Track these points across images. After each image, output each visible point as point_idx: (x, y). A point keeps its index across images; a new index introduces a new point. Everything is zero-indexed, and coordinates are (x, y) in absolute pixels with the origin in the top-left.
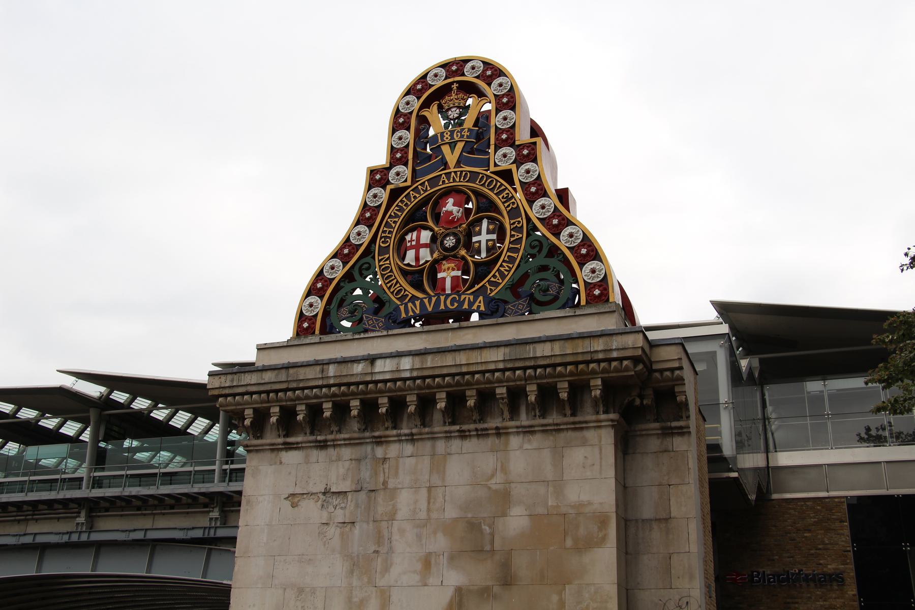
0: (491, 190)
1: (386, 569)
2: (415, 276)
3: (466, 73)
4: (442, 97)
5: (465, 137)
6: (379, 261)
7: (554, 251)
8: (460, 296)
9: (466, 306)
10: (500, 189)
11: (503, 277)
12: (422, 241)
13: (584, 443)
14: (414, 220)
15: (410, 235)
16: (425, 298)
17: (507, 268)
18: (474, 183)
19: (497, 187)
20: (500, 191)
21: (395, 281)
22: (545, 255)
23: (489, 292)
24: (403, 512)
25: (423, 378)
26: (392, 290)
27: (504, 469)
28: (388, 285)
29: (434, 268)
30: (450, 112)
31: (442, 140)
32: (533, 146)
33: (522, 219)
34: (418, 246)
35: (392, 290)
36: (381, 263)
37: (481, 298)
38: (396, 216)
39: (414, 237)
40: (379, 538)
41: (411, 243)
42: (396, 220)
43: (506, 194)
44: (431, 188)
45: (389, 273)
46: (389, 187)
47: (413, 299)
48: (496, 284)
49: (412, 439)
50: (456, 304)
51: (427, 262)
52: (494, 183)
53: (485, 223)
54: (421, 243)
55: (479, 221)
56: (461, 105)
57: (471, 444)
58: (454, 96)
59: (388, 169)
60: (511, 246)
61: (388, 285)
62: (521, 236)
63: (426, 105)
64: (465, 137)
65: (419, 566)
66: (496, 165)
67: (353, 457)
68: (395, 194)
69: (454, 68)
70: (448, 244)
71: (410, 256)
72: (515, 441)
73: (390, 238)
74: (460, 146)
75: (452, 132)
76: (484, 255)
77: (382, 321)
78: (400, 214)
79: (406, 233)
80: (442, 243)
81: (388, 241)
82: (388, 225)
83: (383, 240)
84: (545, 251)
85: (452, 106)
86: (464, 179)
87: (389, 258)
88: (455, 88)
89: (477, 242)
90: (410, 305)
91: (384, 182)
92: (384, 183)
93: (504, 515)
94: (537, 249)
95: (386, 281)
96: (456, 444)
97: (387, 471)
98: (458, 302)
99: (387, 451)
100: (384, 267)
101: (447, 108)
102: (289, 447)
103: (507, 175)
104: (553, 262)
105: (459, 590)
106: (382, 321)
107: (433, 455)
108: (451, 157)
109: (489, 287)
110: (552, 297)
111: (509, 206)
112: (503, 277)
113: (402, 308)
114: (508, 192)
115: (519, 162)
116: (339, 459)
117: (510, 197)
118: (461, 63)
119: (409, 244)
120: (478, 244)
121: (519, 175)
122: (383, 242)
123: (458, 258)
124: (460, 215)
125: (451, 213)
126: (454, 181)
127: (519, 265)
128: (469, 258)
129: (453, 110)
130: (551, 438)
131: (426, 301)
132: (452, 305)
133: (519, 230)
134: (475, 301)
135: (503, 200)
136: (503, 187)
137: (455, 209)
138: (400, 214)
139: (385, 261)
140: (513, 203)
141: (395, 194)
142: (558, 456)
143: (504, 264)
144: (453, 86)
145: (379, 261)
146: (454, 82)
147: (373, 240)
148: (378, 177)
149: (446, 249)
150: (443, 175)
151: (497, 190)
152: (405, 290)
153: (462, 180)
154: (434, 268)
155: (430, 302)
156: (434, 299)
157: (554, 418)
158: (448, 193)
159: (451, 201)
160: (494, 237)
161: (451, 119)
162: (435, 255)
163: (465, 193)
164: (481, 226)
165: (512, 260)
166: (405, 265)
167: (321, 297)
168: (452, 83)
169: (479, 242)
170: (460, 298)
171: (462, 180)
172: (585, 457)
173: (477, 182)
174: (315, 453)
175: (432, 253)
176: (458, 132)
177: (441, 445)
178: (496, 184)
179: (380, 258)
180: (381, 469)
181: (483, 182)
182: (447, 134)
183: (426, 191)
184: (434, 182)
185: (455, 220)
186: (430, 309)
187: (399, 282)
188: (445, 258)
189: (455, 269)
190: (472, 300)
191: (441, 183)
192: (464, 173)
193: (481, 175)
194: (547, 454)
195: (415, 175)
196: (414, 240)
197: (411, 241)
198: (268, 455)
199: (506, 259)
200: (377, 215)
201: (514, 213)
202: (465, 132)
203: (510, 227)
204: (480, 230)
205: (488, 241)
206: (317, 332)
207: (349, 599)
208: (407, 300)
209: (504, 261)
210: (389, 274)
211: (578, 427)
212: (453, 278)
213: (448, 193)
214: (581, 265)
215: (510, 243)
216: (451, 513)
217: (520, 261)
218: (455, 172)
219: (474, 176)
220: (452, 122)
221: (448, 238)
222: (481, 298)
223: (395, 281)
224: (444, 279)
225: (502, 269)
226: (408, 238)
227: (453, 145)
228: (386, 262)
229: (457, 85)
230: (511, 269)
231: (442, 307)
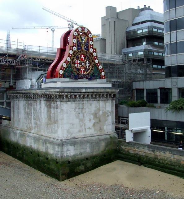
1: (84, 121)
7: (98, 69)
11: (91, 72)
13: (108, 102)
24: (87, 112)
27: (99, 106)
34: (78, 63)
40: (84, 116)
49: (87, 101)
55: (87, 61)
57: (95, 102)
65: (89, 120)
68: (74, 52)
71: (76, 65)
72: (100, 102)
74: (84, 46)
80: (81, 64)
82: (73, 58)
93: (99, 112)
96: (93, 102)
102: (69, 101)
103: (92, 54)
105: (94, 123)
107: (90, 103)
108: (83, 47)
128: (86, 68)
133: (93, 64)
141: (74, 52)
147: (71, 61)
149: (82, 65)
157: (105, 99)
159: (83, 56)
160: (89, 64)
165: (92, 69)
174: (73, 102)
177: (91, 102)
184: (80, 52)
194: (104, 104)
195: (78, 49)
198: (65, 102)
207: (80, 125)
211: (108, 100)
216: (93, 112)
219: (87, 52)
224: (82, 71)
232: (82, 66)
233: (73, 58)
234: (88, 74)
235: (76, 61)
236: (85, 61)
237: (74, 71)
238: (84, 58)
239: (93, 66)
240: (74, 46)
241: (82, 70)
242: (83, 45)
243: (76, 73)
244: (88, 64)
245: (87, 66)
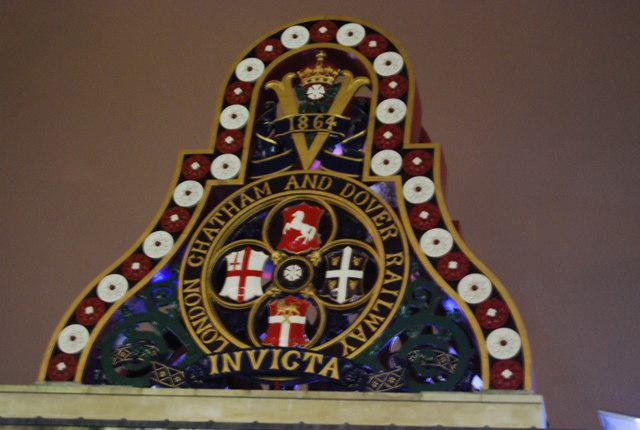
0: (363, 208)
2: (234, 317)
4: (302, 68)
5: (330, 128)
6: (185, 287)
8: (303, 351)
9: (310, 369)
11: (369, 333)
12: (252, 266)
14: (247, 234)
15: (234, 254)
16: (248, 349)
17: (376, 322)
21: (204, 319)
23: (345, 353)
26: (199, 331)
28: (195, 324)
29: (265, 311)
30: (310, 91)
31: (296, 127)
33: (404, 254)
34: (244, 273)
35: (199, 331)
36: (187, 290)
37: (334, 360)
38: (218, 226)
39: (240, 260)
42: (216, 230)
44: (273, 193)
46: (210, 183)
47: (231, 349)
48: (358, 344)
50: (296, 365)
51: (256, 298)
52: (367, 198)
53: (348, 252)
55: (338, 251)
58: (319, 69)
59: (211, 158)
60: (385, 291)
61: (195, 324)
62: (399, 278)
63: (276, 75)
64: (330, 128)
68: (218, 194)
69: (323, 30)
71: (231, 288)
73: (204, 256)
76: (341, 298)
77: (179, 375)
78: (222, 223)
82: (202, 237)
83: (193, 257)
85: (313, 81)
87: (198, 285)
89: (333, 279)
90: (226, 357)
92: (204, 177)
95: (192, 318)
98: (299, 361)
100: (189, 296)
101: (306, 83)
106: (179, 375)
109: (346, 346)
112: (369, 333)
113: (214, 359)
115: (406, 174)
119: (230, 268)
123: (302, 298)
125: (298, 233)
126: (308, 187)
129: (314, 86)
131: (251, 354)
132: (290, 365)
133: (399, 270)
134: (326, 361)
135: (379, 225)
136: (379, 206)
138: (222, 223)
139: (194, 287)
140: (393, 231)
141: (218, 194)
143: (373, 316)
145: (185, 287)
146: (322, 49)
147: (176, 258)
148: (195, 166)
149: (285, 283)
150: (293, 178)
152: (220, 335)
153: (319, 187)
154: (265, 311)
155: (257, 356)
156: (263, 353)
158: (294, 205)
159: (299, 215)
160: (359, 274)
162: (274, 290)
163: (322, 207)
164: (340, 255)
165: (384, 312)
167: (90, 329)
168: (319, 50)
170: (302, 355)
171: (319, 187)
173: (342, 193)
175: (264, 288)
178: (369, 201)
179: (186, 282)
183: (263, 196)
186: (256, 366)
188: (283, 295)
190: (320, 361)
191: (287, 188)
192: (324, 178)
193: (348, 185)
195: (251, 171)
197: (235, 264)
199: (376, 309)
200: (186, 222)
201: (393, 245)
205: (350, 279)
206: (79, 375)
208: (220, 349)
209: (372, 312)
210: (198, 308)
212: (295, 328)
213: (294, 205)
214: (486, 332)
215: (385, 286)
218: (311, 176)
222: (334, 360)
223: (204, 319)
224: (278, 326)
225: (368, 322)
226: (230, 258)
227: (310, 137)
228: (194, 290)
230: (381, 323)
231: (275, 366)
232: (283, 295)
234: (336, 350)
235: (230, 258)
236: (316, 257)
237: (204, 328)
238: (308, 232)
239: (396, 286)
240: (217, 153)
241: (286, 320)
242: (310, 137)
244: (344, 274)
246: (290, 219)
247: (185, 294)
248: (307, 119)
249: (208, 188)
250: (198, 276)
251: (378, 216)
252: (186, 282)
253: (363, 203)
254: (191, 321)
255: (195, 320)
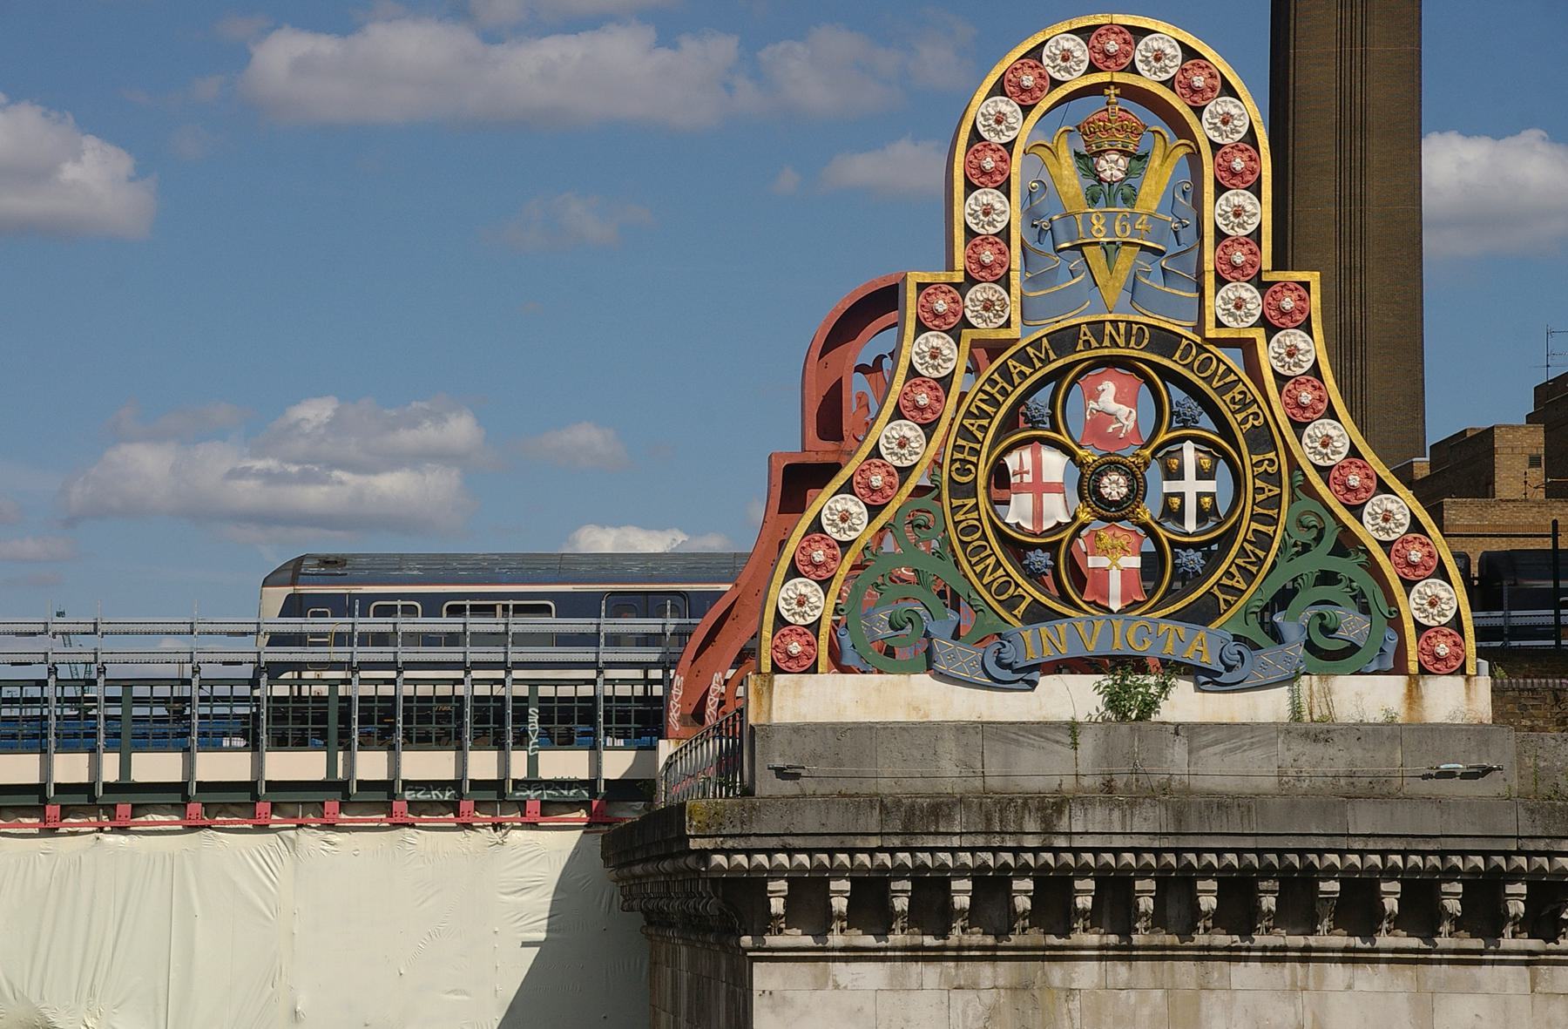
3: (1140, 66)
7: (1347, 544)
10: (1228, 380)
13: (1474, 988)
18: (1170, 357)
19: (1220, 371)
20: (1226, 384)
22: (1329, 550)
25: (1178, 852)
32: (1303, 293)
34: (1040, 488)
39: (1028, 465)
41: (1022, 478)
43: (1239, 393)
45: (978, 540)
51: (1059, 527)
53: (1189, 449)
54: (1044, 481)
56: (1131, 148)
66: (1219, 324)
67: (1001, 982)
70: (1108, 490)
75: (1111, 217)
76: (1190, 525)
79: (1008, 450)
81: (969, 470)
84: (1329, 541)
86: (1138, 343)
88: (1113, 96)
91: (954, 320)
94: (1314, 533)
95: (974, 560)
97: (1076, 1015)
99: (1073, 975)
104: (1344, 567)
110: (1345, 645)
111: (1245, 420)
114: (1245, 389)
115: (1269, 327)
116: (974, 987)
117: (1248, 401)
118: (1128, 36)
120: (1176, 501)
121: (1268, 356)
122: (957, 469)
124: (1130, 424)
127: (1274, 564)
130: (1409, 973)
136: (1232, 377)
137: (1122, 410)
142: (1424, 1008)
144: (1107, 92)
145: (954, 510)
146: (1112, 83)
151: (1217, 382)
159: (1109, 389)
161: (1100, 180)
166: (1008, 525)
168: (1107, 85)
169: (1181, 495)
172: (1477, 1015)
173: (1177, 357)
176: (1125, 218)
179: (956, 503)
180: (1065, 1011)
181: (1190, 359)
182: (1098, 218)
185: (1122, 436)
187: (1001, 565)
189: (1129, 552)
193: (1185, 342)
194: (1401, 1002)
196: (1027, 473)
197: (1021, 473)
202: (1141, 224)
203: (1253, 471)
204: (1181, 468)
205: (1199, 495)
212: (1125, 573)
214: (1408, 585)
217: (1277, 555)
220: (1106, 185)
221: (1116, 477)
227: (1111, 249)
228: (969, 516)
229: (1118, 91)
233: (964, 432)
235: (1012, 461)
240: (971, 281)
243: (1010, 604)
245: (1179, 517)
246: (1095, 396)
247: (956, 524)
248: (1102, 221)
249: (965, 344)
250: (976, 497)
251: (1231, 394)
252: (956, 503)
253: (1209, 372)
254: (972, 566)
255: (977, 563)
